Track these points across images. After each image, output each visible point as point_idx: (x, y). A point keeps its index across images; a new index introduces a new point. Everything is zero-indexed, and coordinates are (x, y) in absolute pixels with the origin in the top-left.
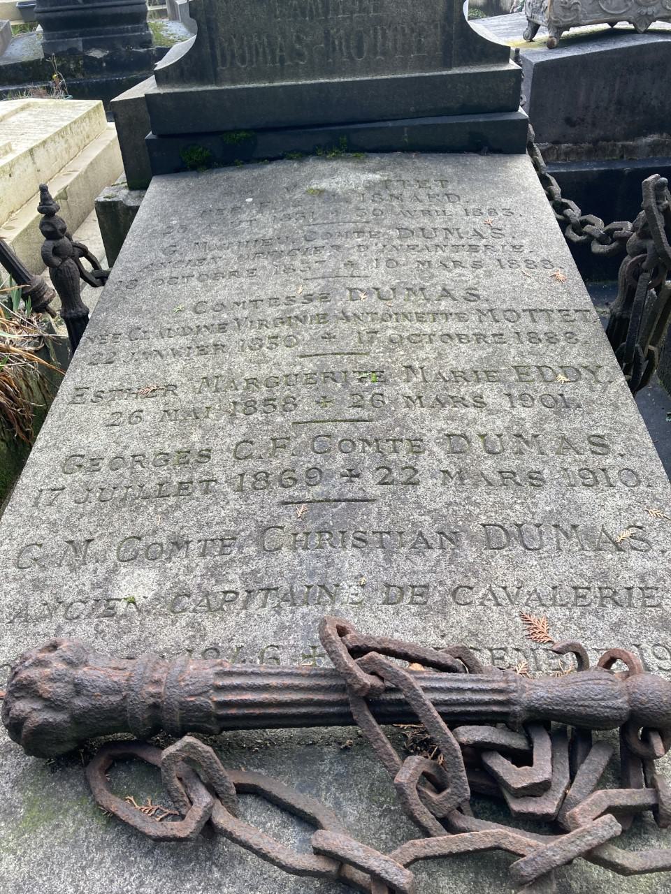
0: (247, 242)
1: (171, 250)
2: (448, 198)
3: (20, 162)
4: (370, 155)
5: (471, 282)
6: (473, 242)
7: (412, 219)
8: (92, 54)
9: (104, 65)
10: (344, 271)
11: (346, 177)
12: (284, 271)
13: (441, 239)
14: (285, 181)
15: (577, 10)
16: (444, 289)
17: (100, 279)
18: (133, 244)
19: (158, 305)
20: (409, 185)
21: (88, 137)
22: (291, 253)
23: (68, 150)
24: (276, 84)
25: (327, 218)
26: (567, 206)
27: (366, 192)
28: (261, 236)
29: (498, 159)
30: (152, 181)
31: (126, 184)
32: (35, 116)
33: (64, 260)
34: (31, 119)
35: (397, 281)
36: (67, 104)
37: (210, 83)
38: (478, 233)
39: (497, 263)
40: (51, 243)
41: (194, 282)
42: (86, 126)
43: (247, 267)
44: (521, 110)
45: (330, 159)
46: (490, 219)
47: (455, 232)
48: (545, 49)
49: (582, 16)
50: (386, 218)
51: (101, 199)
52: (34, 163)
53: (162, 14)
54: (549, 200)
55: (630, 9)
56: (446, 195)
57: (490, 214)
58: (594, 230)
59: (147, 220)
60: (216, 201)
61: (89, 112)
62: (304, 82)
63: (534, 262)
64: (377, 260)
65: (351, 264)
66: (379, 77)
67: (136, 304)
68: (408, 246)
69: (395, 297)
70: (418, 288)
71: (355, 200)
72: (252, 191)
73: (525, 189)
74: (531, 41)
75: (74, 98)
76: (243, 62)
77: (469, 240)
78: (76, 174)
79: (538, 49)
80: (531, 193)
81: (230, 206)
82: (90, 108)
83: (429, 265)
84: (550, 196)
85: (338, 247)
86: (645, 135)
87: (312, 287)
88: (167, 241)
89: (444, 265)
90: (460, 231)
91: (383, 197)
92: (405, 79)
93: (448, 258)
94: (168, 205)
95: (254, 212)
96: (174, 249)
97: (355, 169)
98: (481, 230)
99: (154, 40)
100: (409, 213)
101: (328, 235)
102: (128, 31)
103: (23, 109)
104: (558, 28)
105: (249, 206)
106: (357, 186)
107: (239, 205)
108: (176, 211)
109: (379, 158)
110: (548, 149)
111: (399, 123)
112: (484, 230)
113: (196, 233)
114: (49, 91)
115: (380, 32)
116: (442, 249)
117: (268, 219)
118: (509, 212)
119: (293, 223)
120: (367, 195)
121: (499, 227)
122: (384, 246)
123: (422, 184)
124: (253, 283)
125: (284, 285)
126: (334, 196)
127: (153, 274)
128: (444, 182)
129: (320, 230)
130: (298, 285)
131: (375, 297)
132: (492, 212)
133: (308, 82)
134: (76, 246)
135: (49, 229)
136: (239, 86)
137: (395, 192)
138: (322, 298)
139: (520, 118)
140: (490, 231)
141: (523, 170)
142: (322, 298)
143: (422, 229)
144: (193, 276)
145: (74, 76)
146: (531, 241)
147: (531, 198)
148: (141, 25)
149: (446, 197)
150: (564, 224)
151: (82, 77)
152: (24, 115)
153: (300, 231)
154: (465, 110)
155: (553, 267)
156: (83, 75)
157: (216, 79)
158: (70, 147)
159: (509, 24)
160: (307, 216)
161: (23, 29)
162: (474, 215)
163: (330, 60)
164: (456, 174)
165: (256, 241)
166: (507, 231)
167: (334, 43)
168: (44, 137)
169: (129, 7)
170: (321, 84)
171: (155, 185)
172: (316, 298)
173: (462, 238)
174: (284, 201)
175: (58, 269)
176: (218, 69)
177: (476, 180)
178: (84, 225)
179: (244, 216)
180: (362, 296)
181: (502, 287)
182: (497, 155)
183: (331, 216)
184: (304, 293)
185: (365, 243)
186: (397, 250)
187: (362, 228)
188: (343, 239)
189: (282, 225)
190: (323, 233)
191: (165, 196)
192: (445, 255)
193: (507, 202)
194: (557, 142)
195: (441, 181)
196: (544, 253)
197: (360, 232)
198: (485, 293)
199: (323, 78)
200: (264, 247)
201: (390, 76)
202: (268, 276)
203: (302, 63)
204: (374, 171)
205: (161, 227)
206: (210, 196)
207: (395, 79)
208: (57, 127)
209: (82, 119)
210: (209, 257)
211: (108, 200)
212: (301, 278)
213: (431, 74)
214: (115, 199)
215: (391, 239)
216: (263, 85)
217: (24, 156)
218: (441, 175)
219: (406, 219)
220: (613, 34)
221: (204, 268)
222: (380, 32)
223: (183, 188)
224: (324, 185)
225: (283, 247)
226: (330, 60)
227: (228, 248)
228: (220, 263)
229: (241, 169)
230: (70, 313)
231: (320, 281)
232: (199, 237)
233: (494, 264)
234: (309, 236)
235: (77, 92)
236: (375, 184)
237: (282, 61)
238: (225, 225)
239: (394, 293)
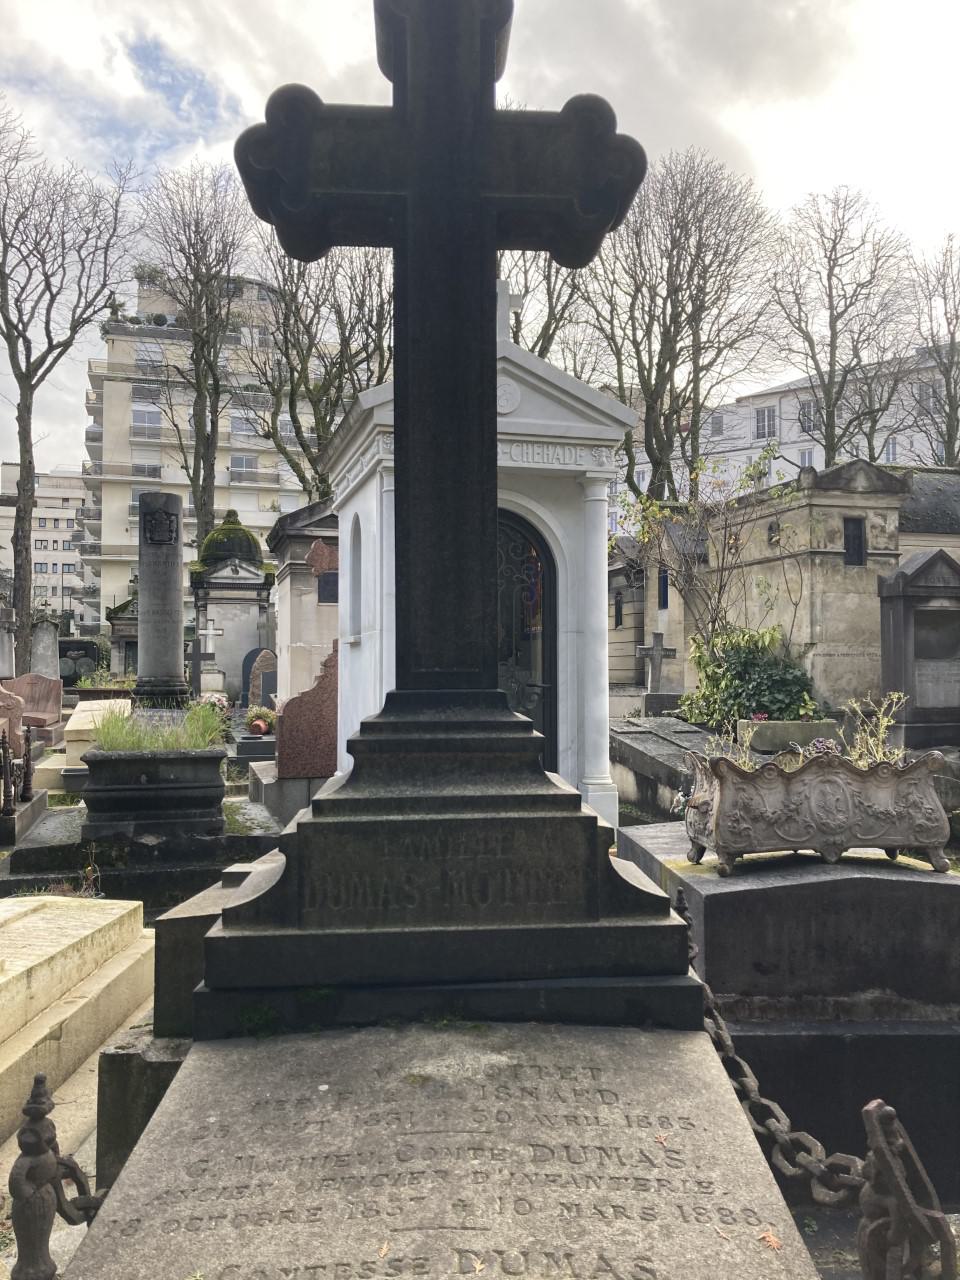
0: (313, 1158)
1: (198, 1170)
2: (602, 1097)
3: (10, 987)
4: (494, 1024)
5: (640, 1245)
6: (640, 1173)
7: (552, 1129)
8: (143, 841)
9: (156, 853)
10: (451, 1218)
11: (461, 1060)
12: (363, 1213)
13: (594, 1165)
14: (377, 1059)
15: (749, 836)
16: (601, 1257)
17: (85, 1211)
18: (147, 1154)
19: (164, 1269)
20: (548, 1074)
21: (113, 949)
22: (376, 1182)
23: (79, 969)
24: (376, 930)
25: (431, 1123)
26: (771, 1114)
27: (487, 1083)
28: (333, 1148)
29: (668, 1037)
30: (192, 1050)
31: (151, 1027)
32: (48, 921)
33: (39, 1186)
34: (41, 924)
35: (531, 1239)
36: (95, 906)
37: (292, 925)
38: (646, 1157)
39: (677, 1213)
40: (28, 1161)
41: (227, 1228)
42: (113, 935)
43: (308, 1203)
44: (691, 973)
45: (441, 1030)
46: (663, 1134)
47: (614, 1154)
48: (715, 877)
49: (756, 842)
50: (514, 1126)
51: (112, 1050)
52: (29, 988)
53: (239, 790)
54: (741, 1100)
55: (812, 837)
56: (600, 1091)
57: (662, 1125)
58: (811, 1162)
59: (172, 1115)
60: (277, 1086)
61: (122, 917)
62: (412, 929)
63: (731, 1213)
64: (500, 1198)
65: (463, 1205)
66: (507, 927)
67: (130, 1264)
68: (547, 1175)
69: (527, 1268)
70: (561, 1253)
71: (473, 1094)
72: (328, 1074)
73: (707, 1086)
74: (698, 863)
75: (108, 896)
76: (337, 903)
77: (634, 1170)
78: (83, 1002)
79: (707, 876)
80: (717, 1093)
81: (295, 1096)
82: (124, 912)
83: (578, 1211)
84: (742, 1094)
85: (444, 1174)
86: (863, 990)
87: (403, 1247)
88: (197, 1152)
89: (601, 1212)
90: (621, 1152)
91: (511, 1092)
92: (541, 930)
93: (605, 1200)
94: (208, 1089)
95: (329, 1108)
96: (203, 1166)
97: (474, 1046)
98: (651, 1152)
99: (226, 826)
100: (544, 1120)
101: (431, 1152)
102: (195, 815)
103: (35, 910)
104: (728, 853)
105: (323, 1097)
106: (476, 1073)
107: (308, 1094)
108: (217, 1101)
109: (506, 1031)
110: (737, 1002)
111: (532, 984)
112: (655, 1152)
113: (241, 1139)
114: (76, 887)
115: (509, 876)
116: (595, 1181)
117: (347, 1121)
118: (687, 1123)
119: (382, 1130)
120: (490, 1088)
121: (676, 1147)
122: (512, 1174)
123: (565, 1072)
124: (313, 1234)
125: (360, 1240)
126: (442, 1087)
127: (165, 1211)
128: (595, 1071)
129: (420, 1143)
130: (381, 1241)
131: (497, 1268)
132: (664, 1122)
133: (418, 929)
134: (61, 1162)
135: (31, 1139)
136: (328, 931)
137: (528, 1084)
138: (417, 1266)
139: (692, 983)
140: (662, 1154)
141: (701, 1055)
142: (417, 1266)
143: (567, 1147)
144: (225, 1217)
145: (113, 865)
146: (723, 1174)
147: (717, 1101)
148: (213, 810)
149: (598, 1096)
150: (767, 1141)
151: (123, 867)
152: (34, 918)
153: (392, 1144)
154: (617, 971)
155: (760, 1222)
156: (125, 864)
157: (300, 922)
158: (85, 963)
159: (670, 837)
160: (402, 1117)
161: (61, 801)
162: (639, 1126)
163: (447, 905)
164: (611, 1059)
165: (326, 1157)
166: (687, 1155)
167: (452, 886)
168: (52, 951)
169: (203, 790)
170: (434, 932)
171: (195, 1057)
172: (407, 1266)
173: (624, 1164)
174: (372, 1092)
175: (28, 1202)
176: (305, 911)
177: (639, 1069)
178: (76, 1077)
179: (313, 1115)
180: (478, 1266)
181: (689, 1256)
182: (665, 1032)
183: (437, 1120)
184: (391, 1256)
185: (483, 1169)
186: (531, 1182)
187: (480, 1142)
188: (453, 1160)
189: (366, 1131)
190: (424, 1147)
191: (205, 1076)
192: (600, 1194)
193: (684, 1106)
194: (746, 994)
195: (591, 1069)
196: (744, 1197)
197: (478, 1149)
198: (663, 1267)
199: (436, 925)
200: (338, 1169)
201: (521, 926)
202: (338, 1222)
203: (411, 906)
204: (498, 1050)
205: (191, 1126)
206: (270, 1079)
207: (527, 930)
208: (74, 937)
209: (112, 925)
210: (255, 1182)
211: (121, 1052)
212: (387, 1227)
213: (573, 925)
214: (131, 1051)
215: (521, 1163)
216: (358, 931)
217: (18, 978)
218: (591, 1060)
219: (543, 1129)
220: (797, 863)
221: (243, 1204)
222: (509, 876)
223: (234, 1065)
224: (430, 1069)
225: (364, 1170)
226: (447, 905)
227: (284, 1169)
228: (269, 1195)
229: (318, 1037)
230: (27, 1274)
231: (416, 1234)
232: (243, 1149)
233: (673, 1214)
234: (405, 1153)
235: (112, 888)
236: (499, 1069)
237: (386, 903)
238: (285, 1128)
239: (526, 1261)
